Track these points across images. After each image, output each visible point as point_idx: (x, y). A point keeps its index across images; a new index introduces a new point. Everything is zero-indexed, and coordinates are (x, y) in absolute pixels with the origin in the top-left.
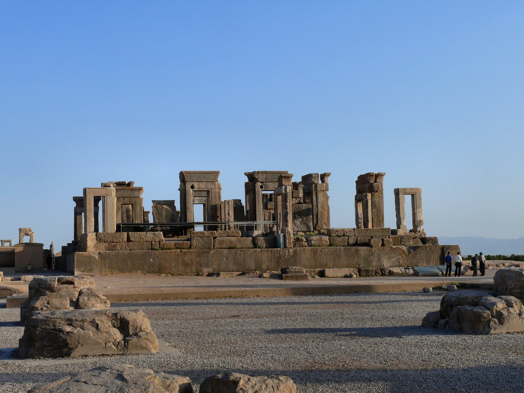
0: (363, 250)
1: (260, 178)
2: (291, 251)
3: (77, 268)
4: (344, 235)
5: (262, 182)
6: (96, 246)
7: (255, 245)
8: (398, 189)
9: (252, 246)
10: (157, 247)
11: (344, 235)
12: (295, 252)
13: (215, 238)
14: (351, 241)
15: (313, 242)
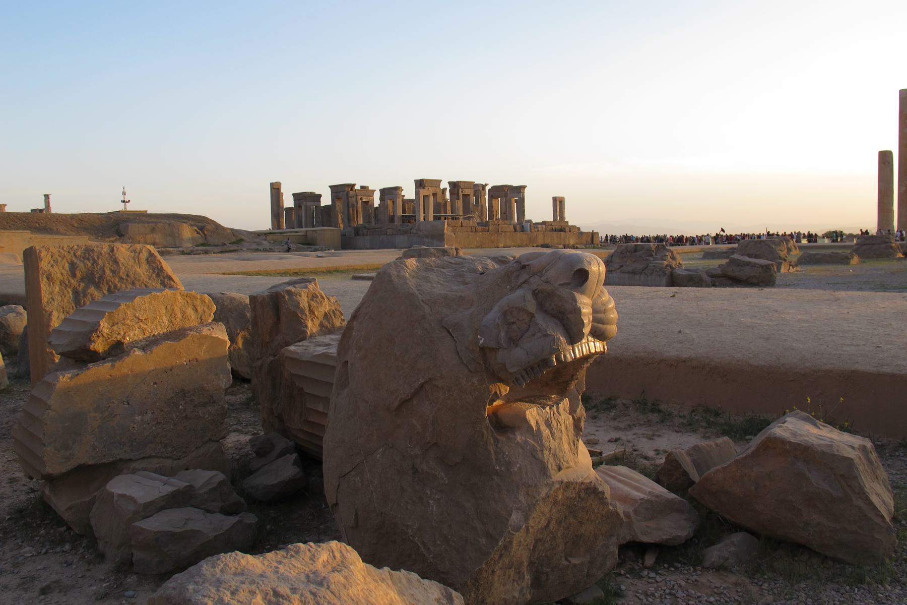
0: (562, 233)
1: (462, 186)
2: (535, 233)
3: (447, 245)
4: (551, 225)
5: (462, 189)
6: (447, 229)
7: (515, 230)
8: (556, 197)
9: (513, 231)
10: (474, 231)
11: (551, 225)
12: (536, 235)
13: (499, 225)
14: (554, 228)
15: (539, 229)
